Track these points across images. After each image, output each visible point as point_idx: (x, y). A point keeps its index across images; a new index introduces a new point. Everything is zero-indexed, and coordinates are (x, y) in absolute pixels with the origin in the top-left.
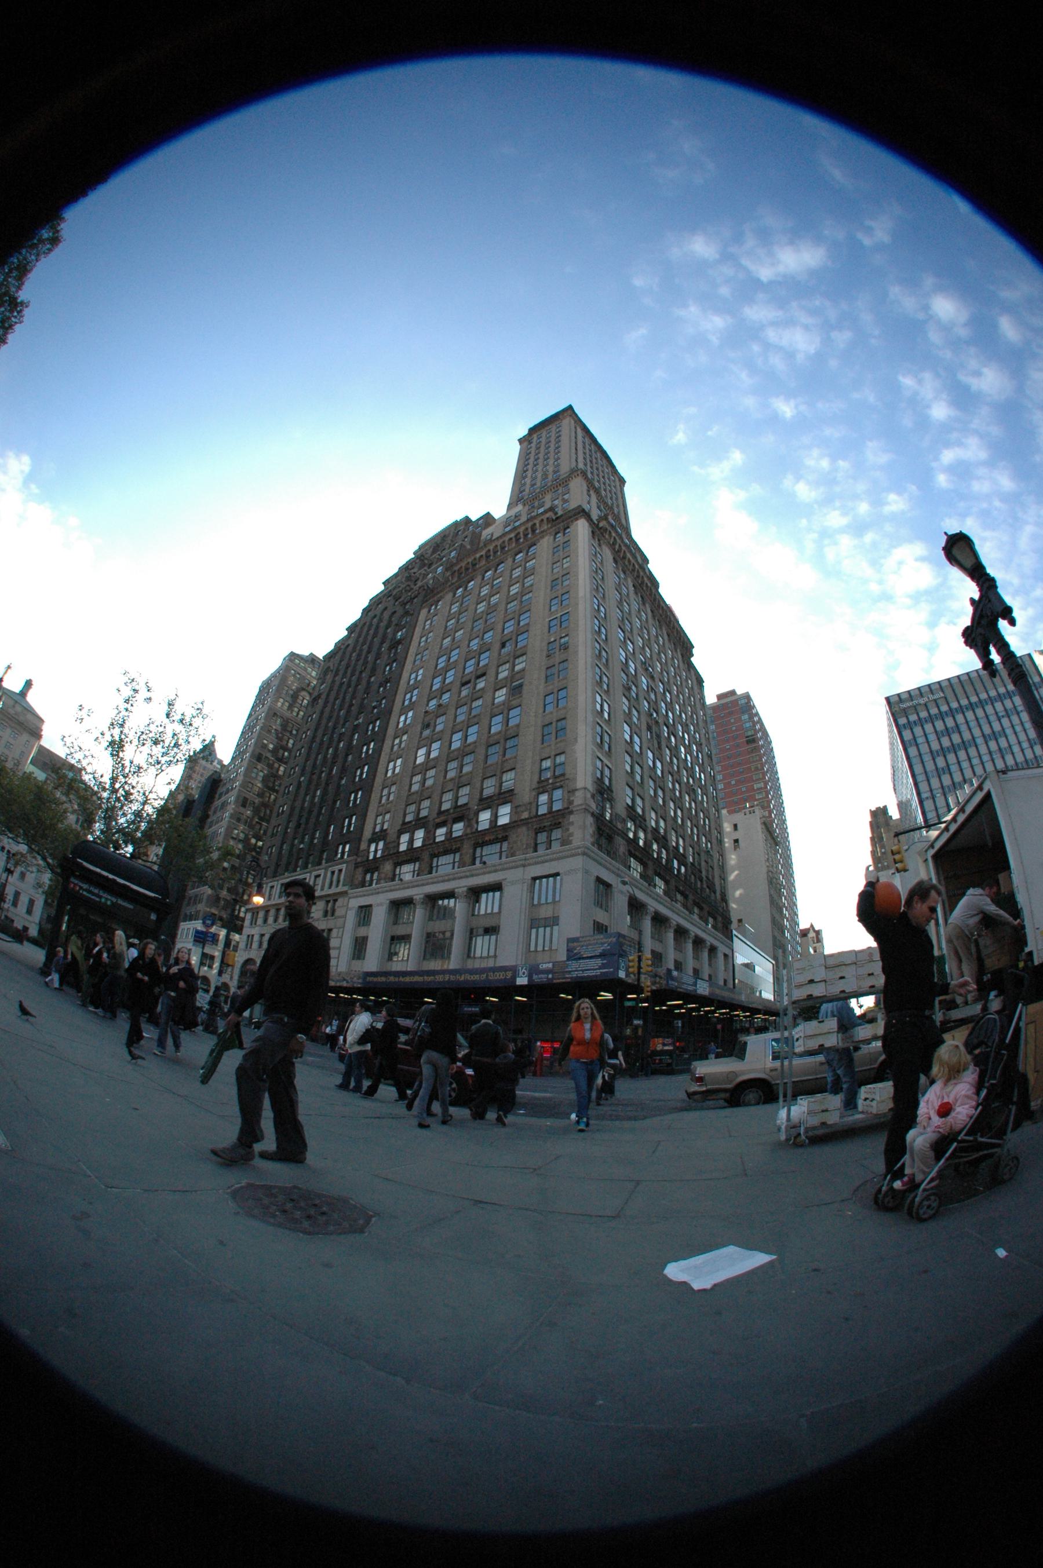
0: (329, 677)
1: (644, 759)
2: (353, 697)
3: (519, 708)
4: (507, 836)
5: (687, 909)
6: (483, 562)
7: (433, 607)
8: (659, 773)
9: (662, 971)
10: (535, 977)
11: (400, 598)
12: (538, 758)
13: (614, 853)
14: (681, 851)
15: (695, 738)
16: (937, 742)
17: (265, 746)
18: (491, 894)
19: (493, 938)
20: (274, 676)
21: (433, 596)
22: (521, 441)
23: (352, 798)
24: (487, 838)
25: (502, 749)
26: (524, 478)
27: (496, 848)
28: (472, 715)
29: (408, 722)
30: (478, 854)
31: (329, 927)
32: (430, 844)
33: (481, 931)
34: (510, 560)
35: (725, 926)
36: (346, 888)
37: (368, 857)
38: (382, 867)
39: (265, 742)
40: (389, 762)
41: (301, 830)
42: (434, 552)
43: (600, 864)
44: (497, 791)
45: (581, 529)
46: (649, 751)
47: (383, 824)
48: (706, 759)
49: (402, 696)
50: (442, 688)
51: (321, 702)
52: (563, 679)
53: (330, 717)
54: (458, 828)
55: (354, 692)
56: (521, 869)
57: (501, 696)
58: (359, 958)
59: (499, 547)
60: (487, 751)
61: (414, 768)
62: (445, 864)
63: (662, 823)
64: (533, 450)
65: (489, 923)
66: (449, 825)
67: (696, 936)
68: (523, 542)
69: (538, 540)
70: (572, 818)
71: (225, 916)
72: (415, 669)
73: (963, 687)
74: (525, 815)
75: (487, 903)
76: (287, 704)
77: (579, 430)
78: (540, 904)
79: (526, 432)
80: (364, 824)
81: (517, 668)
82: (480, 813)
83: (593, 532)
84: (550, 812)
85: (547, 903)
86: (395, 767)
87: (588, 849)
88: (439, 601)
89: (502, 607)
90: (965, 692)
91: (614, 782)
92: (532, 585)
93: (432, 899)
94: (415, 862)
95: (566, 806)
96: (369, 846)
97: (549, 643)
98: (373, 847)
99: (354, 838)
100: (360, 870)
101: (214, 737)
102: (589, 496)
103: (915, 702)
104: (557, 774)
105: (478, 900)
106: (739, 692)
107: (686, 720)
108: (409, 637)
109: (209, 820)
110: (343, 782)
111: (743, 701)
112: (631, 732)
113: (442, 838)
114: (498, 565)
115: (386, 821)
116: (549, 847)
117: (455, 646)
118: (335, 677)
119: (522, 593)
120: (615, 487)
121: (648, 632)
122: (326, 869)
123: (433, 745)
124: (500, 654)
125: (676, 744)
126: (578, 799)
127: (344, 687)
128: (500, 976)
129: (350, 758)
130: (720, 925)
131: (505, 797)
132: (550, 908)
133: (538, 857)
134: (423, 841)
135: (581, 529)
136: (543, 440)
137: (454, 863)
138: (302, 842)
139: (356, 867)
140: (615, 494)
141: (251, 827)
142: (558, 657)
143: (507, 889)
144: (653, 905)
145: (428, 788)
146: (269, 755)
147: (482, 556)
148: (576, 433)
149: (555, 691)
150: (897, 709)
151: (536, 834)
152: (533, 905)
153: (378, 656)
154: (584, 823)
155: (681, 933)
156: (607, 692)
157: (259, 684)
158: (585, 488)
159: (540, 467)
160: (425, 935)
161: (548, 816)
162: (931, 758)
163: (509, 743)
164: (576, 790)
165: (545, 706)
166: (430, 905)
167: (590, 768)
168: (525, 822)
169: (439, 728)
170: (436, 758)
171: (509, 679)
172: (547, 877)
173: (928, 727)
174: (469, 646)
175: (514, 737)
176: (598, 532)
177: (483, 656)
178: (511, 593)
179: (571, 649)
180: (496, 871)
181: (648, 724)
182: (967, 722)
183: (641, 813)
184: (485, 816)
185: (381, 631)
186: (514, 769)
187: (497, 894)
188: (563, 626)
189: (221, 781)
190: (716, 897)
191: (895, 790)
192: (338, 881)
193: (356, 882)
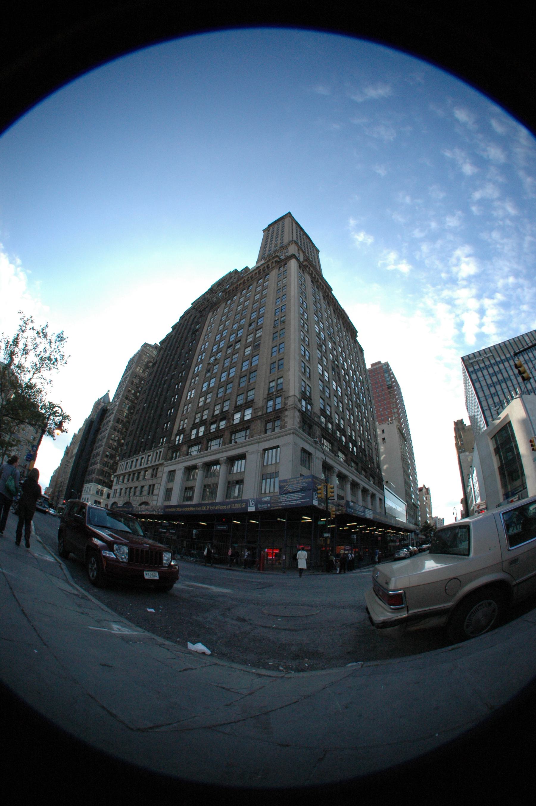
0: (162, 352)
2: (173, 361)
3: (258, 356)
4: (249, 426)
5: (358, 472)
6: (242, 286)
8: (340, 394)
12: (267, 381)
16: (490, 379)
17: (129, 391)
20: (135, 355)
22: (264, 231)
23: (169, 413)
24: (238, 428)
25: (247, 378)
26: (265, 248)
27: (243, 433)
28: (233, 362)
29: (199, 370)
30: (233, 438)
31: (153, 484)
32: (207, 434)
34: (255, 283)
35: (380, 483)
36: (162, 462)
37: (175, 443)
39: (130, 389)
41: (143, 432)
42: (218, 287)
43: (304, 440)
45: (293, 264)
46: (333, 381)
47: (183, 425)
49: (197, 357)
50: (217, 350)
51: (157, 365)
53: (161, 372)
54: (223, 424)
55: (174, 358)
56: (257, 445)
57: (248, 351)
58: (168, 501)
60: (240, 380)
61: (201, 393)
62: (214, 445)
63: (342, 422)
64: (270, 235)
66: (218, 423)
67: (364, 488)
68: (263, 274)
69: (270, 272)
70: (287, 413)
71: (107, 481)
72: (204, 343)
73: (502, 349)
74: (260, 413)
75: (239, 467)
76: (142, 369)
77: (294, 225)
78: (267, 465)
79: (267, 226)
81: (257, 336)
83: (299, 266)
84: (274, 410)
85: (272, 464)
86: (191, 394)
87: (296, 430)
88: (218, 308)
89: (251, 306)
90: (503, 353)
91: (312, 395)
93: (208, 465)
94: (199, 445)
95: (283, 406)
96: (176, 438)
99: (168, 434)
100: (170, 451)
101: (109, 391)
102: (299, 254)
104: (278, 389)
105: (232, 465)
106: (382, 362)
107: (354, 368)
108: (202, 328)
109: (101, 431)
111: (385, 367)
112: (322, 369)
113: (214, 430)
114: (249, 287)
115: (186, 424)
116: (274, 430)
117: (225, 329)
119: (261, 298)
120: (314, 253)
121: (332, 320)
122: (154, 451)
124: (248, 329)
126: (290, 402)
130: (377, 482)
131: (248, 404)
132: (274, 467)
134: (204, 432)
135: (293, 264)
136: (275, 229)
137: (220, 444)
139: (168, 450)
141: (122, 433)
142: (279, 327)
143: (248, 457)
144: (338, 468)
146: (132, 396)
147: (241, 283)
148: (292, 225)
149: (278, 345)
151: (266, 424)
152: (264, 466)
155: (354, 485)
156: (308, 345)
157: (128, 360)
158: (297, 249)
159: (273, 242)
160: (203, 486)
161: (273, 413)
162: (487, 388)
163: (253, 375)
164: (289, 397)
167: (297, 385)
168: (260, 417)
170: (213, 387)
172: (272, 448)
173: (485, 372)
175: (255, 371)
176: (302, 266)
178: (256, 299)
179: (286, 323)
180: (243, 447)
181: (332, 367)
182: (505, 368)
183: (329, 414)
184: (238, 416)
185: (189, 326)
186: (254, 389)
189: (107, 410)
190: (374, 466)
192: (159, 457)
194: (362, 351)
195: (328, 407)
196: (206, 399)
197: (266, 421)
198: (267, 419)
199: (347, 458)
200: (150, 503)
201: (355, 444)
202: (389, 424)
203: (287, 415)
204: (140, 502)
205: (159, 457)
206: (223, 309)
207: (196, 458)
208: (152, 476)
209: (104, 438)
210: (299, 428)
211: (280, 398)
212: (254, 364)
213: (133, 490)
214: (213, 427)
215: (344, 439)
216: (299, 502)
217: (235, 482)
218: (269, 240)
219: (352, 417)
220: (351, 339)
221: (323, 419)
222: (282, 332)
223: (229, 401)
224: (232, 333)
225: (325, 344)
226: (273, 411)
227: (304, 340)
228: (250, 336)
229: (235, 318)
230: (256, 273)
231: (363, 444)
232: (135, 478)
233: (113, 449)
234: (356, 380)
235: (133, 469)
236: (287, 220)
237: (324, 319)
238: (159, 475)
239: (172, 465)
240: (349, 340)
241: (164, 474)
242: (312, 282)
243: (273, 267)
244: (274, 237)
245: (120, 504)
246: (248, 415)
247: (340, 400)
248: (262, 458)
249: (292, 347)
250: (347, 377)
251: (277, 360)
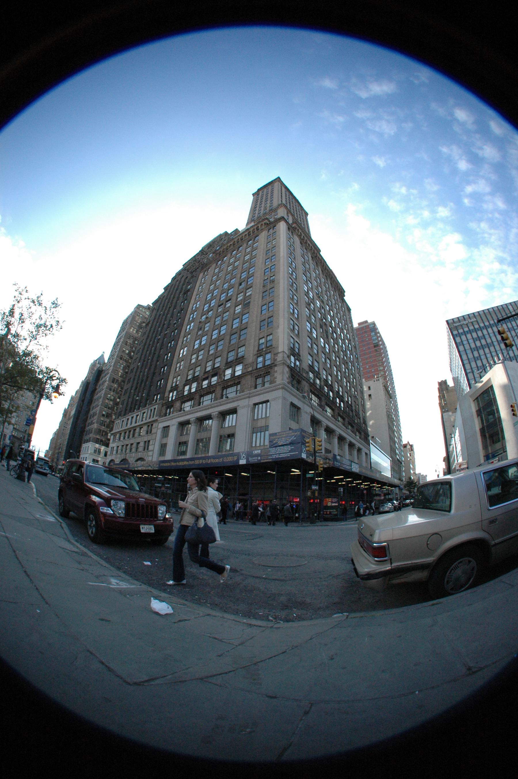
0: (155, 312)
1: (319, 343)
2: (165, 320)
3: (248, 314)
4: (240, 382)
5: (345, 427)
6: (232, 247)
8: (327, 351)
9: (330, 456)
12: (257, 338)
13: (302, 390)
14: (341, 394)
15: (347, 337)
17: (124, 351)
20: (129, 317)
22: (253, 195)
24: (229, 384)
25: (238, 335)
26: (255, 211)
27: (234, 389)
29: (191, 328)
30: (224, 393)
32: (199, 390)
35: (365, 437)
36: (157, 418)
37: (169, 400)
39: (124, 349)
41: (137, 390)
42: (208, 248)
44: (235, 358)
45: (282, 226)
46: (321, 339)
48: (353, 349)
49: (189, 316)
50: (208, 309)
51: (150, 325)
52: (272, 297)
53: (154, 332)
54: (214, 380)
55: (166, 317)
56: (248, 399)
57: (238, 309)
59: (240, 240)
60: (230, 338)
61: (193, 351)
62: (207, 400)
63: (330, 378)
64: (260, 199)
66: (209, 379)
67: (350, 442)
68: (252, 235)
70: (276, 368)
71: (104, 440)
74: (250, 369)
75: (230, 420)
76: (136, 330)
77: (283, 188)
78: (258, 419)
79: (256, 190)
80: (167, 383)
81: (247, 294)
82: (226, 371)
84: (264, 366)
85: (262, 418)
87: (285, 385)
91: (301, 352)
92: (256, 254)
93: (201, 420)
94: (191, 401)
95: (272, 362)
96: (169, 395)
97: (264, 280)
98: (171, 394)
99: (162, 391)
100: (165, 407)
101: (104, 353)
102: (288, 216)
103: (461, 323)
104: (268, 345)
105: (224, 420)
106: (369, 321)
107: (342, 327)
109: (97, 391)
111: (372, 326)
113: (206, 386)
114: (239, 248)
121: (320, 280)
122: (148, 409)
126: (280, 358)
130: (363, 437)
131: (239, 360)
132: (263, 421)
134: (196, 389)
135: (282, 226)
136: (265, 193)
137: (212, 399)
138: (138, 396)
139: (162, 406)
140: (303, 219)
141: (117, 393)
143: (239, 411)
144: (325, 422)
145: (199, 360)
146: (126, 356)
147: (231, 245)
148: (281, 189)
149: (267, 303)
150: (452, 326)
151: (256, 379)
155: (341, 439)
156: (297, 304)
157: (122, 321)
159: (263, 205)
161: (262, 368)
163: (242, 332)
164: (279, 353)
165: (262, 311)
166: (199, 424)
167: (286, 342)
168: (250, 373)
169: (206, 329)
171: (243, 300)
172: (262, 403)
174: (223, 287)
175: (245, 329)
176: (290, 228)
178: (245, 259)
179: (276, 282)
180: (234, 401)
181: (320, 325)
183: (317, 370)
184: (229, 372)
185: (180, 287)
186: (244, 345)
189: (103, 371)
190: (360, 421)
191: (451, 370)
192: (154, 414)
194: (349, 310)
195: (316, 364)
196: (198, 357)
197: (256, 376)
198: (257, 375)
199: (334, 413)
200: (145, 458)
201: (342, 400)
202: (375, 381)
203: (276, 371)
204: (136, 459)
205: (154, 414)
206: (213, 269)
207: (190, 413)
208: (147, 433)
209: (100, 398)
210: (288, 383)
211: (270, 354)
212: (244, 322)
213: (129, 446)
214: (205, 383)
215: (331, 394)
217: (227, 436)
218: (258, 203)
219: (339, 373)
220: (339, 299)
221: (311, 375)
222: (271, 291)
223: (220, 358)
224: (223, 292)
225: (313, 302)
226: (263, 367)
227: (293, 299)
228: (240, 295)
229: (225, 278)
230: (246, 235)
231: (350, 399)
232: (131, 436)
233: (109, 408)
234: (344, 337)
235: (129, 426)
236: (276, 184)
237: (313, 278)
238: (154, 431)
240: (337, 299)
241: (158, 430)
242: (301, 242)
243: (262, 229)
244: (264, 200)
245: (117, 461)
246: (239, 370)
247: (328, 357)
248: (253, 412)
249: (281, 305)
250: (335, 335)
251: (267, 317)
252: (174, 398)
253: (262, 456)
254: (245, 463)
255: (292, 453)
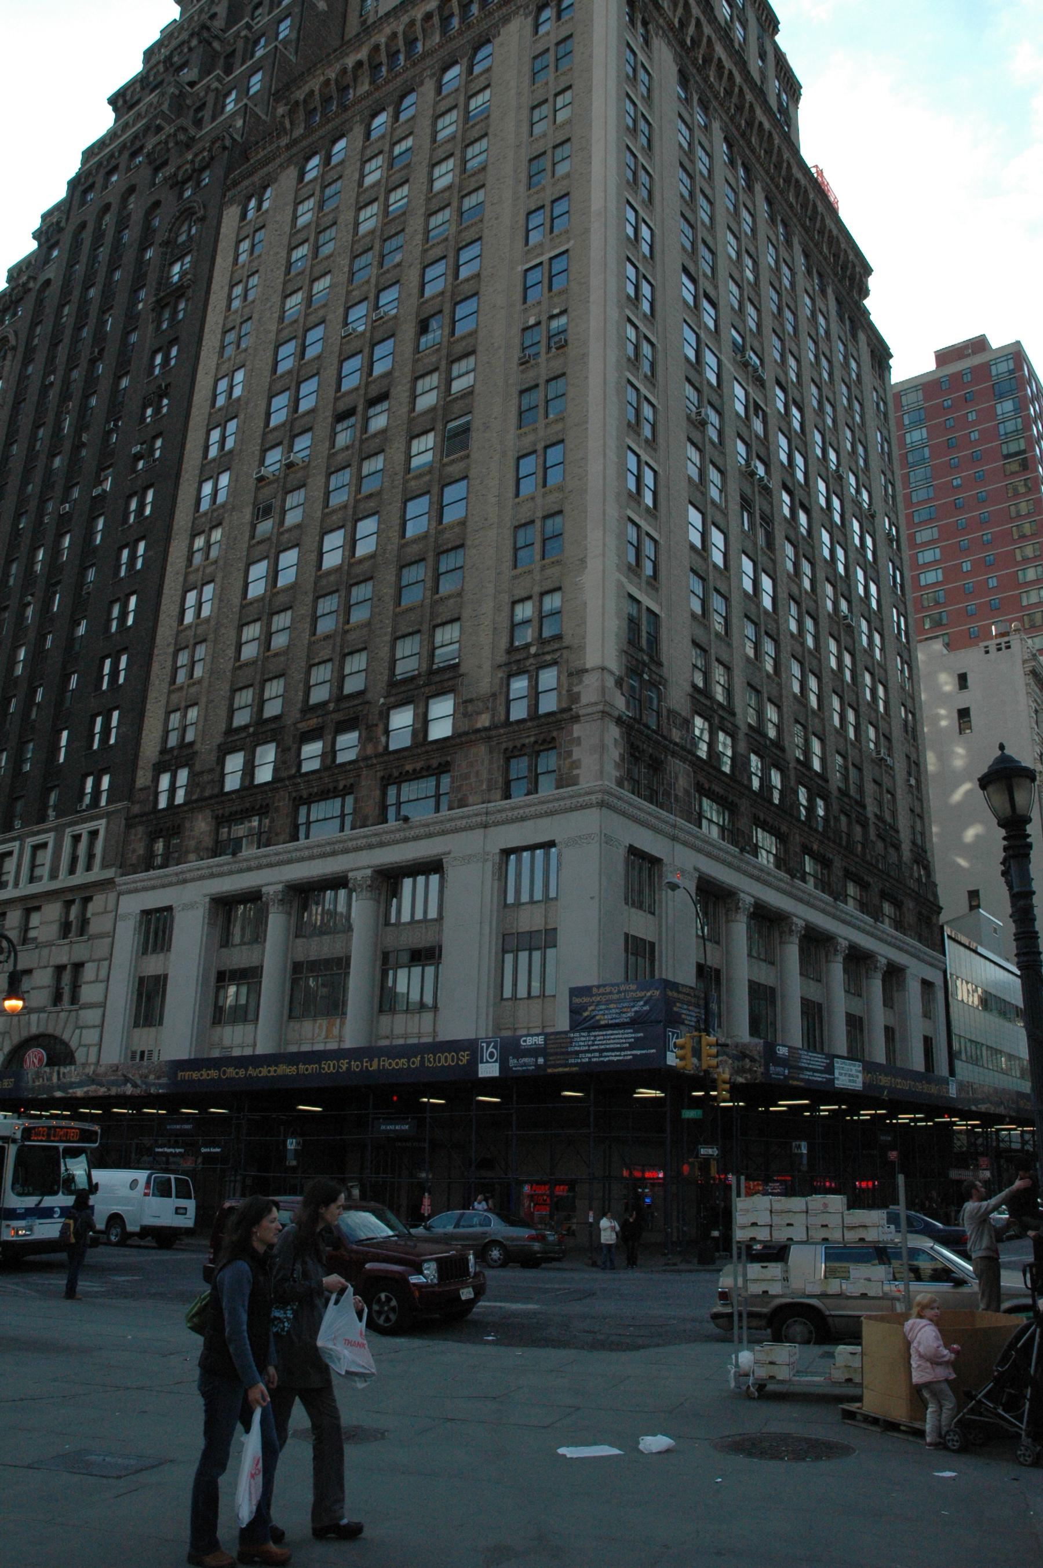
2: (80, 426)
6: (364, 87)
7: (253, 203)
10: (512, 1062)
11: (165, 163)
12: (506, 599)
13: (666, 793)
18: (421, 879)
19: (430, 970)
21: (251, 174)
24: (409, 767)
27: (428, 785)
30: (391, 799)
32: (291, 777)
33: (405, 958)
34: (429, 85)
36: (109, 873)
37: (156, 802)
38: (187, 825)
40: (186, 592)
52: (557, 421)
60: (399, 577)
65: (421, 939)
68: (461, 32)
70: (577, 730)
74: (484, 721)
78: (518, 904)
81: (457, 386)
82: (392, 712)
85: (532, 902)
88: (265, 188)
92: (483, 169)
95: (564, 705)
96: (156, 781)
104: (546, 634)
107: (838, 466)
110: (81, 630)
111: (1003, 367)
114: (403, 97)
118: (25, 364)
119: (463, 189)
121: (755, 263)
122: (59, 830)
123: (282, 556)
124: (417, 350)
125: (809, 531)
126: (589, 691)
127: (53, 394)
128: (446, 1060)
129: (91, 575)
130: (910, 918)
132: (539, 911)
133: (513, 809)
137: (343, 816)
139: (129, 826)
142: (544, 368)
147: (359, 64)
149: (540, 447)
151: (508, 760)
152: (506, 905)
153: (131, 322)
154: (602, 740)
156: (652, 444)
160: (289, 966)
163: (447, 563)
164: (587, 671)
165: (518, 480)
166: (295, 905)
168: (485, 735)
169: (293, 518)
170: (293, 587)
171: (440, 412)
172: (532, 848)
174: (346, 324)
177: (379, 351)
179: (572, 350)
184: (402, 719)
186: (458, 619)
187: (434, 879)
188: (556, 287)
190: (900, 857)
192: (91, 856)
193: (134, 860)
197: (506, 749)
198: (510, 745)
199: (786, 851)
202: (993, 649)
203: (579, 738)
208: (65, 928)
214: (312, 749)
216: (628, 1055)
239: (154, 888)
242: (684, 79)
248: (499, 879)
251: (540, 514)
252: (180, 797)
253: (552, 1055)
254: (497, 1074)
255: (638, 1052)
